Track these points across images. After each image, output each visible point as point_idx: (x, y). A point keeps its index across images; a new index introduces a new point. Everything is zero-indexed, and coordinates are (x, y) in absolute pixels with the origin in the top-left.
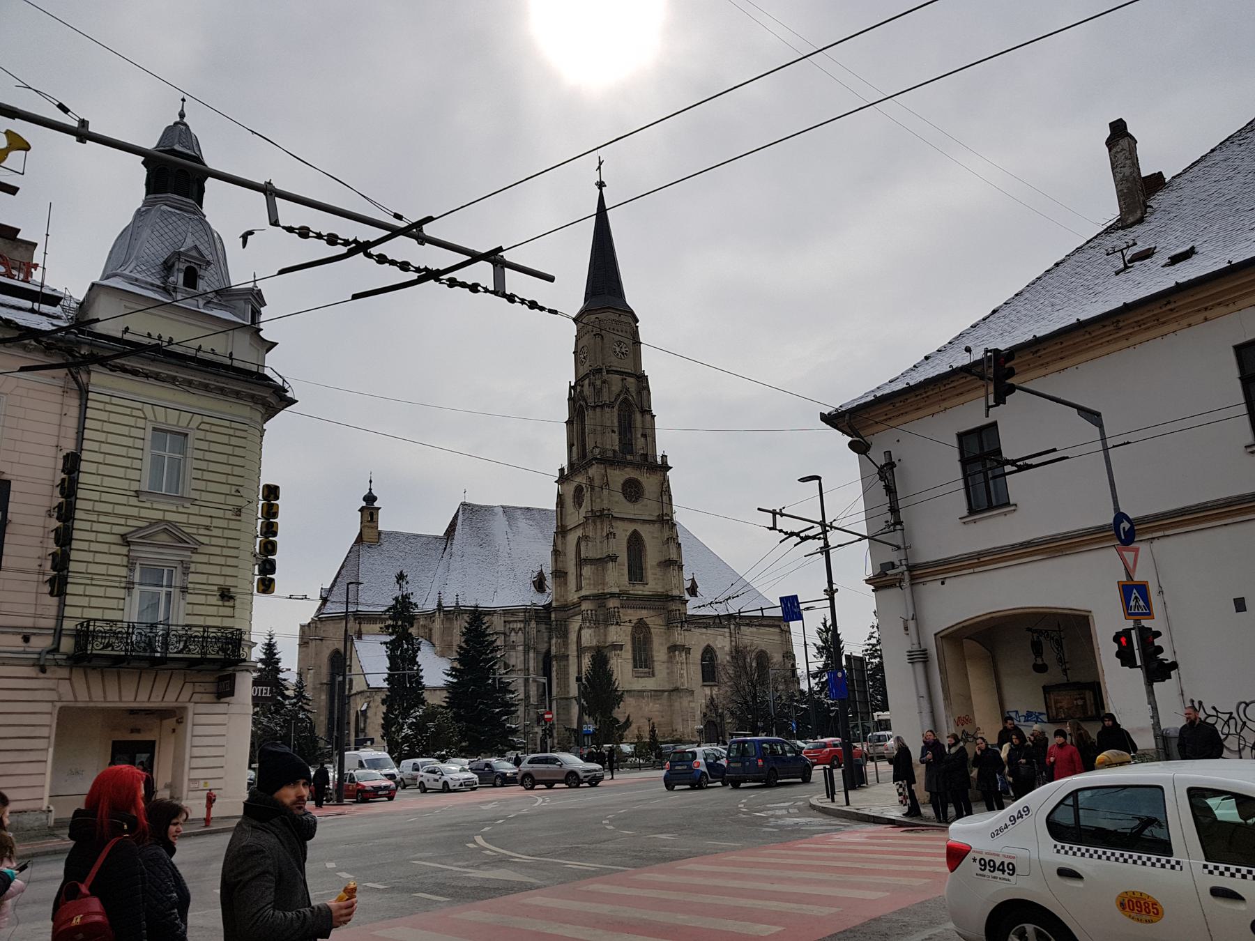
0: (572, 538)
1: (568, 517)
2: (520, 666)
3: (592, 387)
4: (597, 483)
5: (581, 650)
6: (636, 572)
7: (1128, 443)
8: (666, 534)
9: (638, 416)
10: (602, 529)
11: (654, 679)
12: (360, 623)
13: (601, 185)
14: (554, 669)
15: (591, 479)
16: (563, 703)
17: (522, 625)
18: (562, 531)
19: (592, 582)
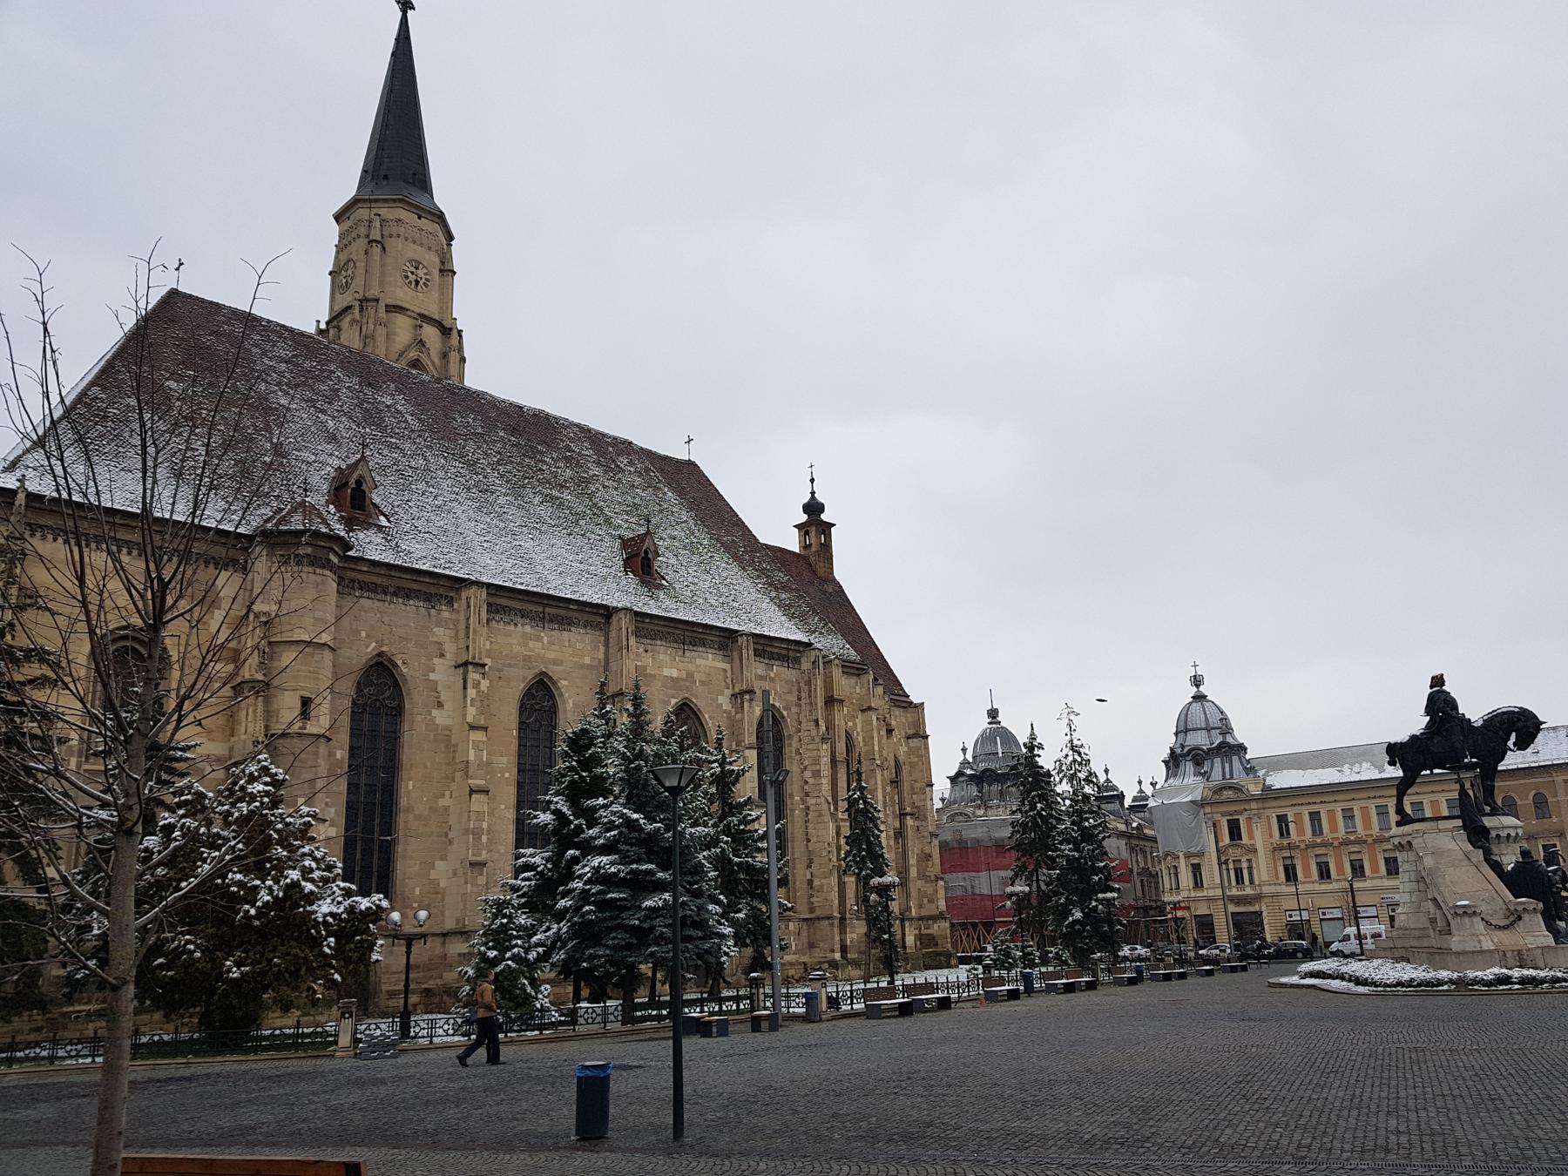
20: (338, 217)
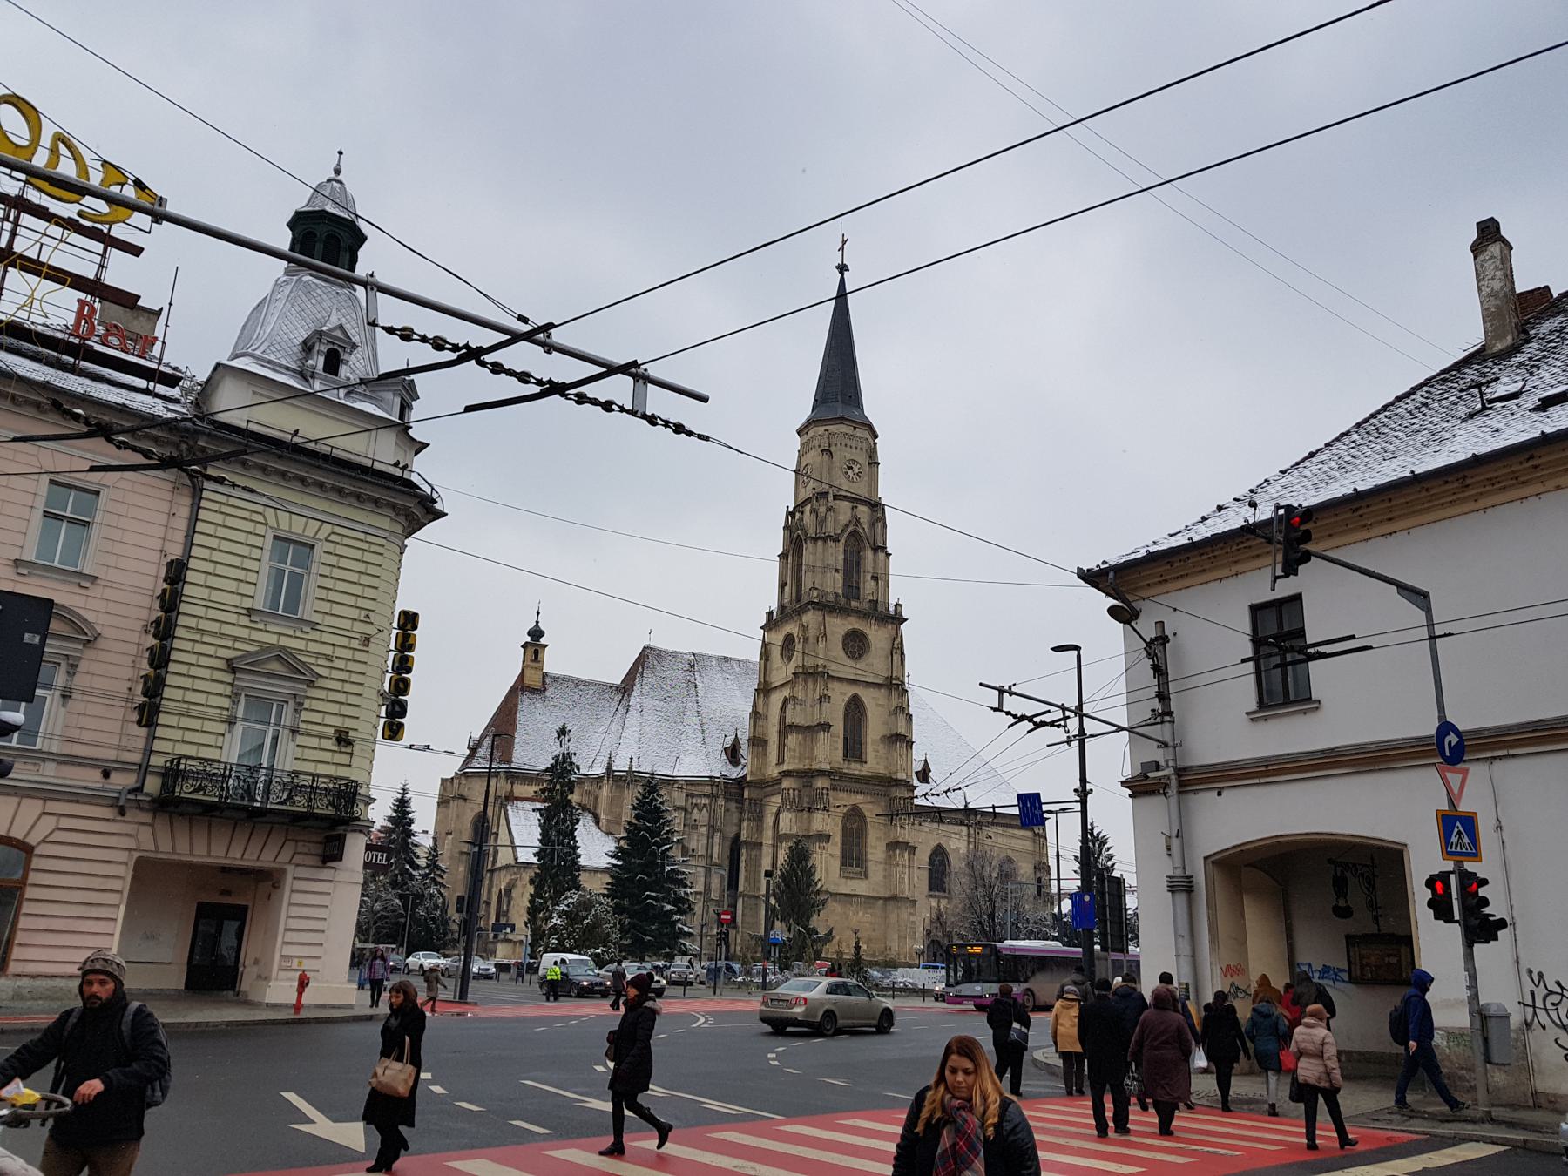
0: (776, 699)
1: (774, 672)
2: (701, 851)
3: (814, 515)
4: (812, 633)
5: (778, 837)
6: (853, 747)
7: (1450, 634)
8: (895, 701)
9: (869, 554)
10: (815, 690)
11: (867, 882)
12: (512, 783)
13: (842, 268)
14: (743, 858)
15: (804, 628)
16: (752, 901)
17: (708, 802)
18: (764, 690)
19: (797, 754)
20: (799, 432)
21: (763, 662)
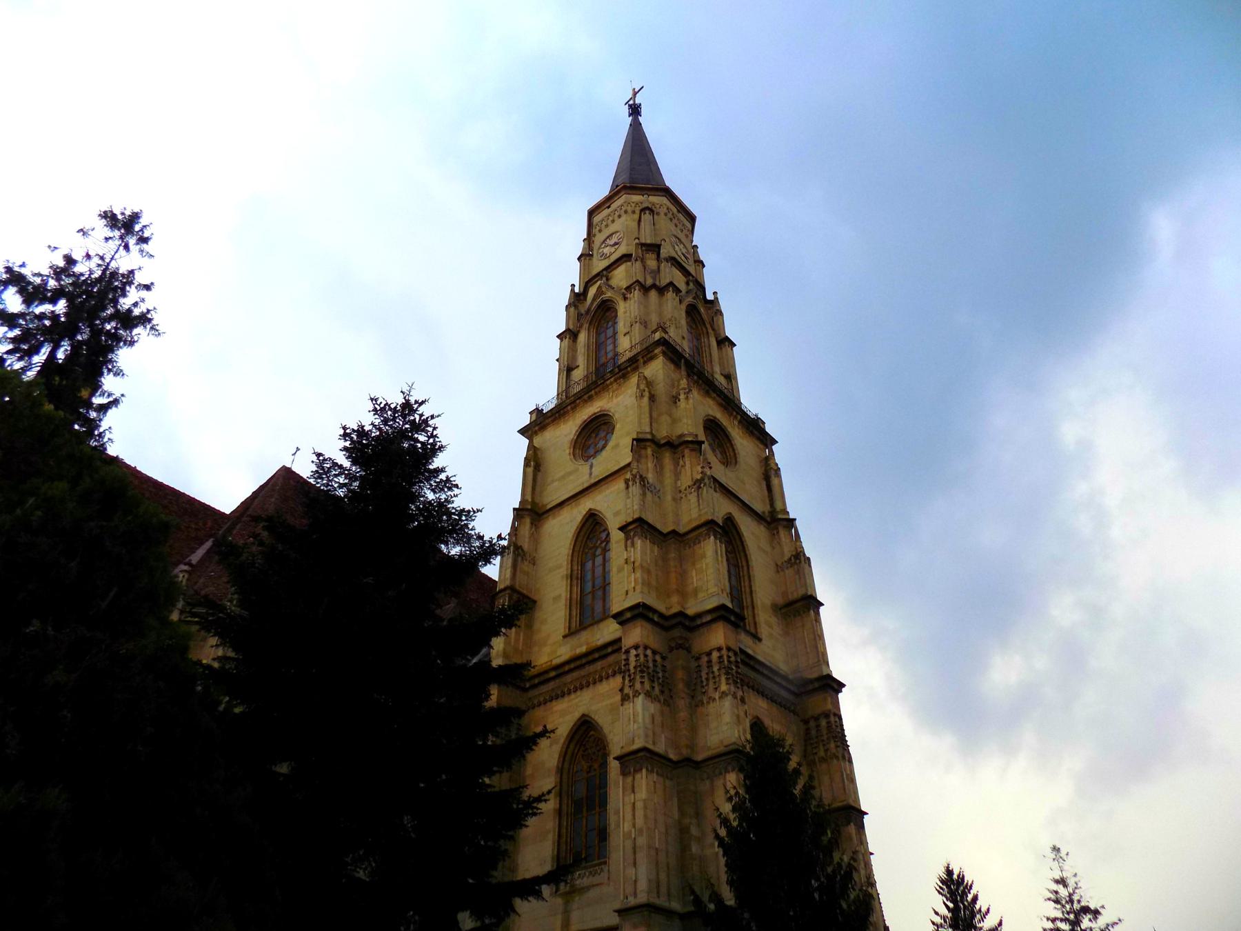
4: (661, 389)
8: (788, 552)
10: (677, 475)
13: (635, 110)
21: (530, 470)
